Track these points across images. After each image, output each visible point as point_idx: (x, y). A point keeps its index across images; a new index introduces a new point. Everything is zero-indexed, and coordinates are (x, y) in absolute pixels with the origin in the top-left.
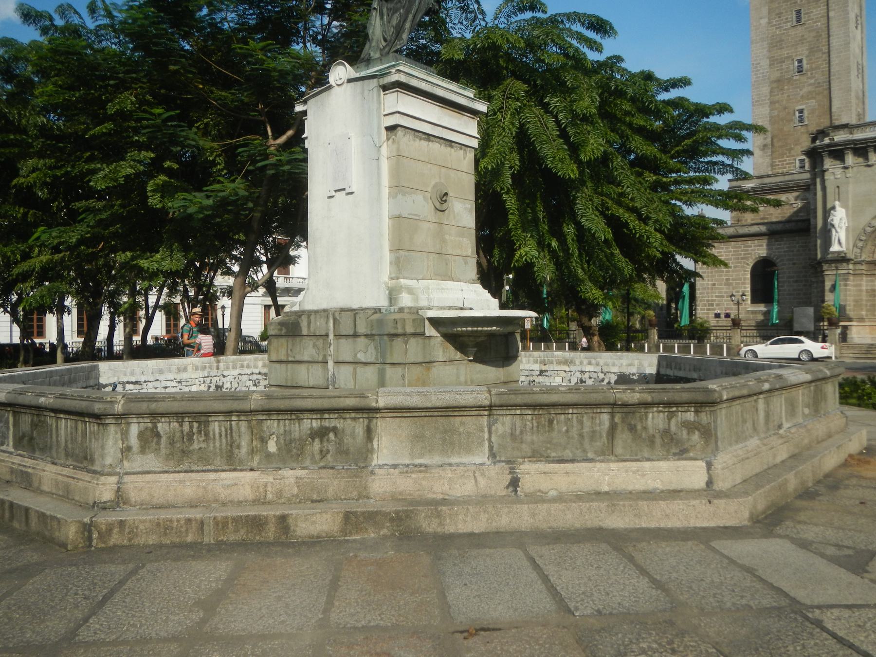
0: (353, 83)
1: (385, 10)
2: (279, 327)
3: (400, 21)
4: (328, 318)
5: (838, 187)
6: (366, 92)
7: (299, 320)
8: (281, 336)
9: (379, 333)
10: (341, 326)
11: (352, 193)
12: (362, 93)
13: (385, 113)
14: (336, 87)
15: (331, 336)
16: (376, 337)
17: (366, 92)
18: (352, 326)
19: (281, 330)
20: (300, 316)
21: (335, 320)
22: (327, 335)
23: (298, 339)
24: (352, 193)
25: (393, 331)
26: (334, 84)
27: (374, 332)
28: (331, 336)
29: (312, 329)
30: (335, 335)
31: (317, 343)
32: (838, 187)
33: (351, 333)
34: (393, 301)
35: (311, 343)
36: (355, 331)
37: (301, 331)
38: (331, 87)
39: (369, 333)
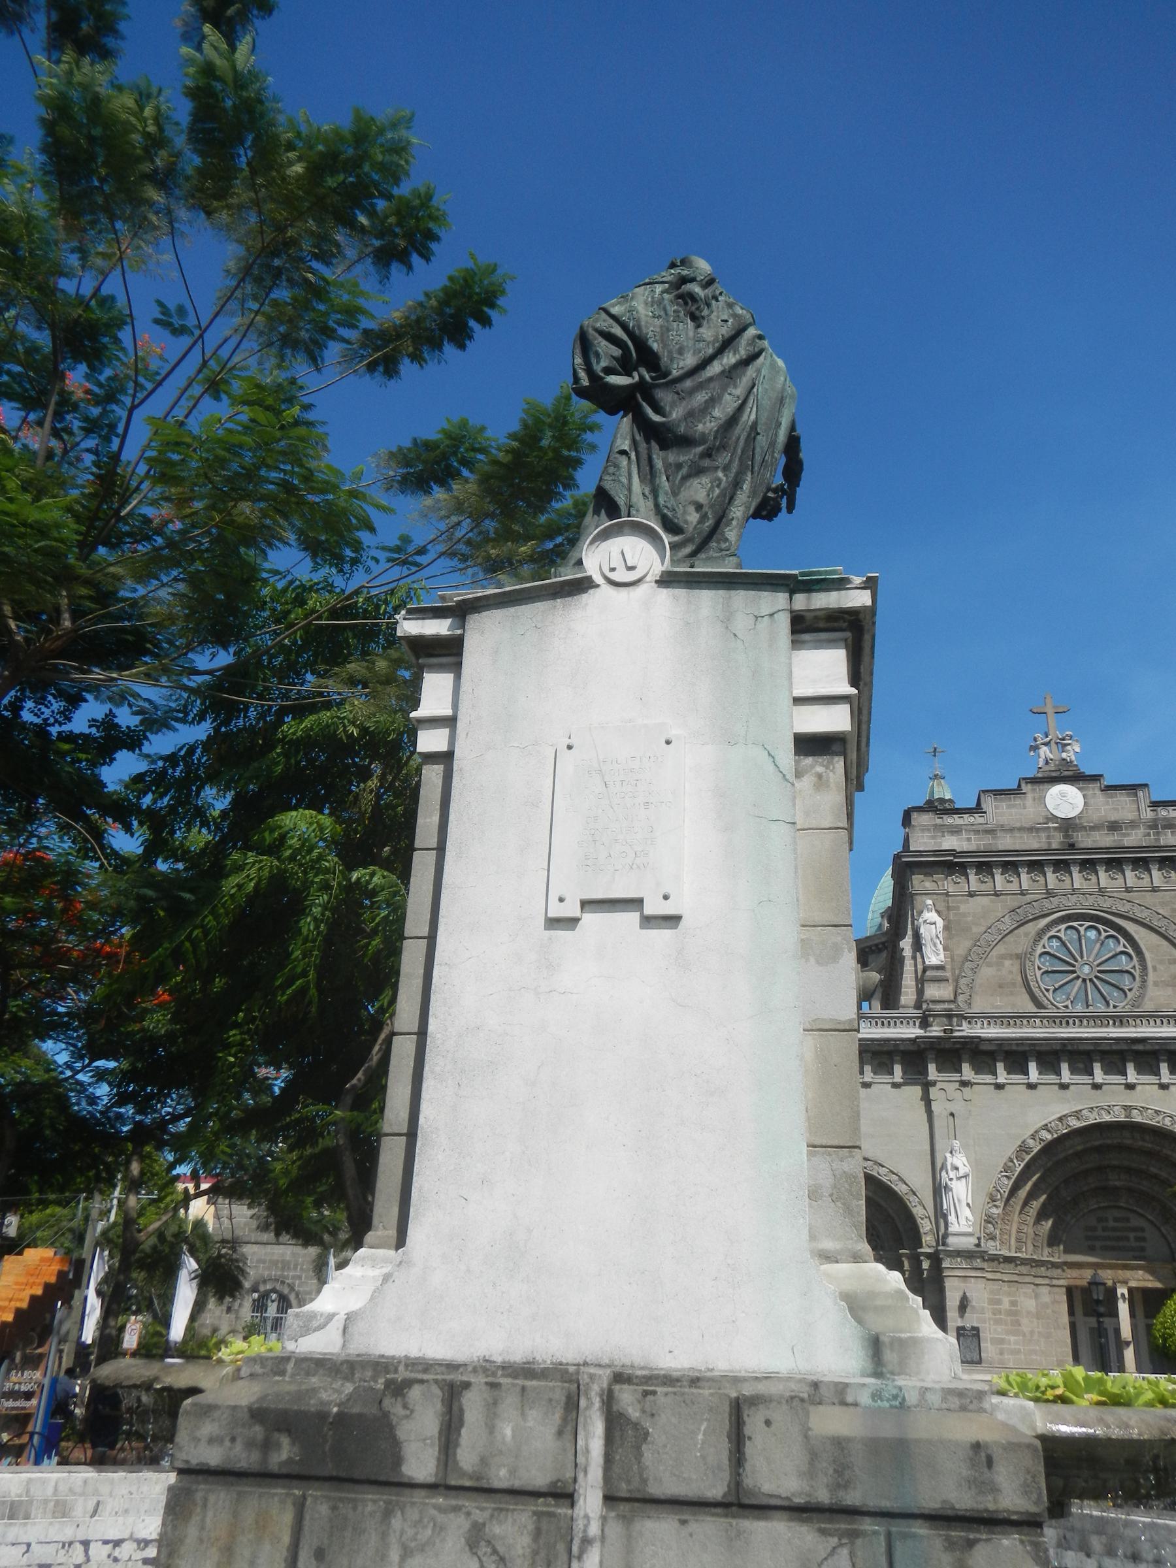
0: (681, 592)
1: (659, 464)
2: (258, 1431)
3: (723, 494)
4: (572, 1406)
5: (952, 1115)
6: (741, 623)
7: (395, 1408)
8: (263, 1476)
9: (886, 1504)
10: (648, 1455)
11: (672, 920)
12: (727, 620)
13: (798, 692)
14: (606, 589)
15: (590, 1501)
16: (867, 1525)
17: (741, 623)
18: (721, 1450)
19: (267, 1446)
20: (398, 1389)
21: (615, 1422)
22: (564, 1495)
23: (371, 1502)
24: (672, 920)
25: (964, 1500)
26: (598, 579)
27: (852, 1498)
28: (590, 1501)
29: (467, 1456)
30: (610, 1499)
31: (497, 1529)
32: (952, 1115)
33: (717, 1490)
34: (889, 1356)
35: (458, 1525)
36: (737, 1483)
37: (398, 1460)
38: (583, 585)
39: (823, 1496)
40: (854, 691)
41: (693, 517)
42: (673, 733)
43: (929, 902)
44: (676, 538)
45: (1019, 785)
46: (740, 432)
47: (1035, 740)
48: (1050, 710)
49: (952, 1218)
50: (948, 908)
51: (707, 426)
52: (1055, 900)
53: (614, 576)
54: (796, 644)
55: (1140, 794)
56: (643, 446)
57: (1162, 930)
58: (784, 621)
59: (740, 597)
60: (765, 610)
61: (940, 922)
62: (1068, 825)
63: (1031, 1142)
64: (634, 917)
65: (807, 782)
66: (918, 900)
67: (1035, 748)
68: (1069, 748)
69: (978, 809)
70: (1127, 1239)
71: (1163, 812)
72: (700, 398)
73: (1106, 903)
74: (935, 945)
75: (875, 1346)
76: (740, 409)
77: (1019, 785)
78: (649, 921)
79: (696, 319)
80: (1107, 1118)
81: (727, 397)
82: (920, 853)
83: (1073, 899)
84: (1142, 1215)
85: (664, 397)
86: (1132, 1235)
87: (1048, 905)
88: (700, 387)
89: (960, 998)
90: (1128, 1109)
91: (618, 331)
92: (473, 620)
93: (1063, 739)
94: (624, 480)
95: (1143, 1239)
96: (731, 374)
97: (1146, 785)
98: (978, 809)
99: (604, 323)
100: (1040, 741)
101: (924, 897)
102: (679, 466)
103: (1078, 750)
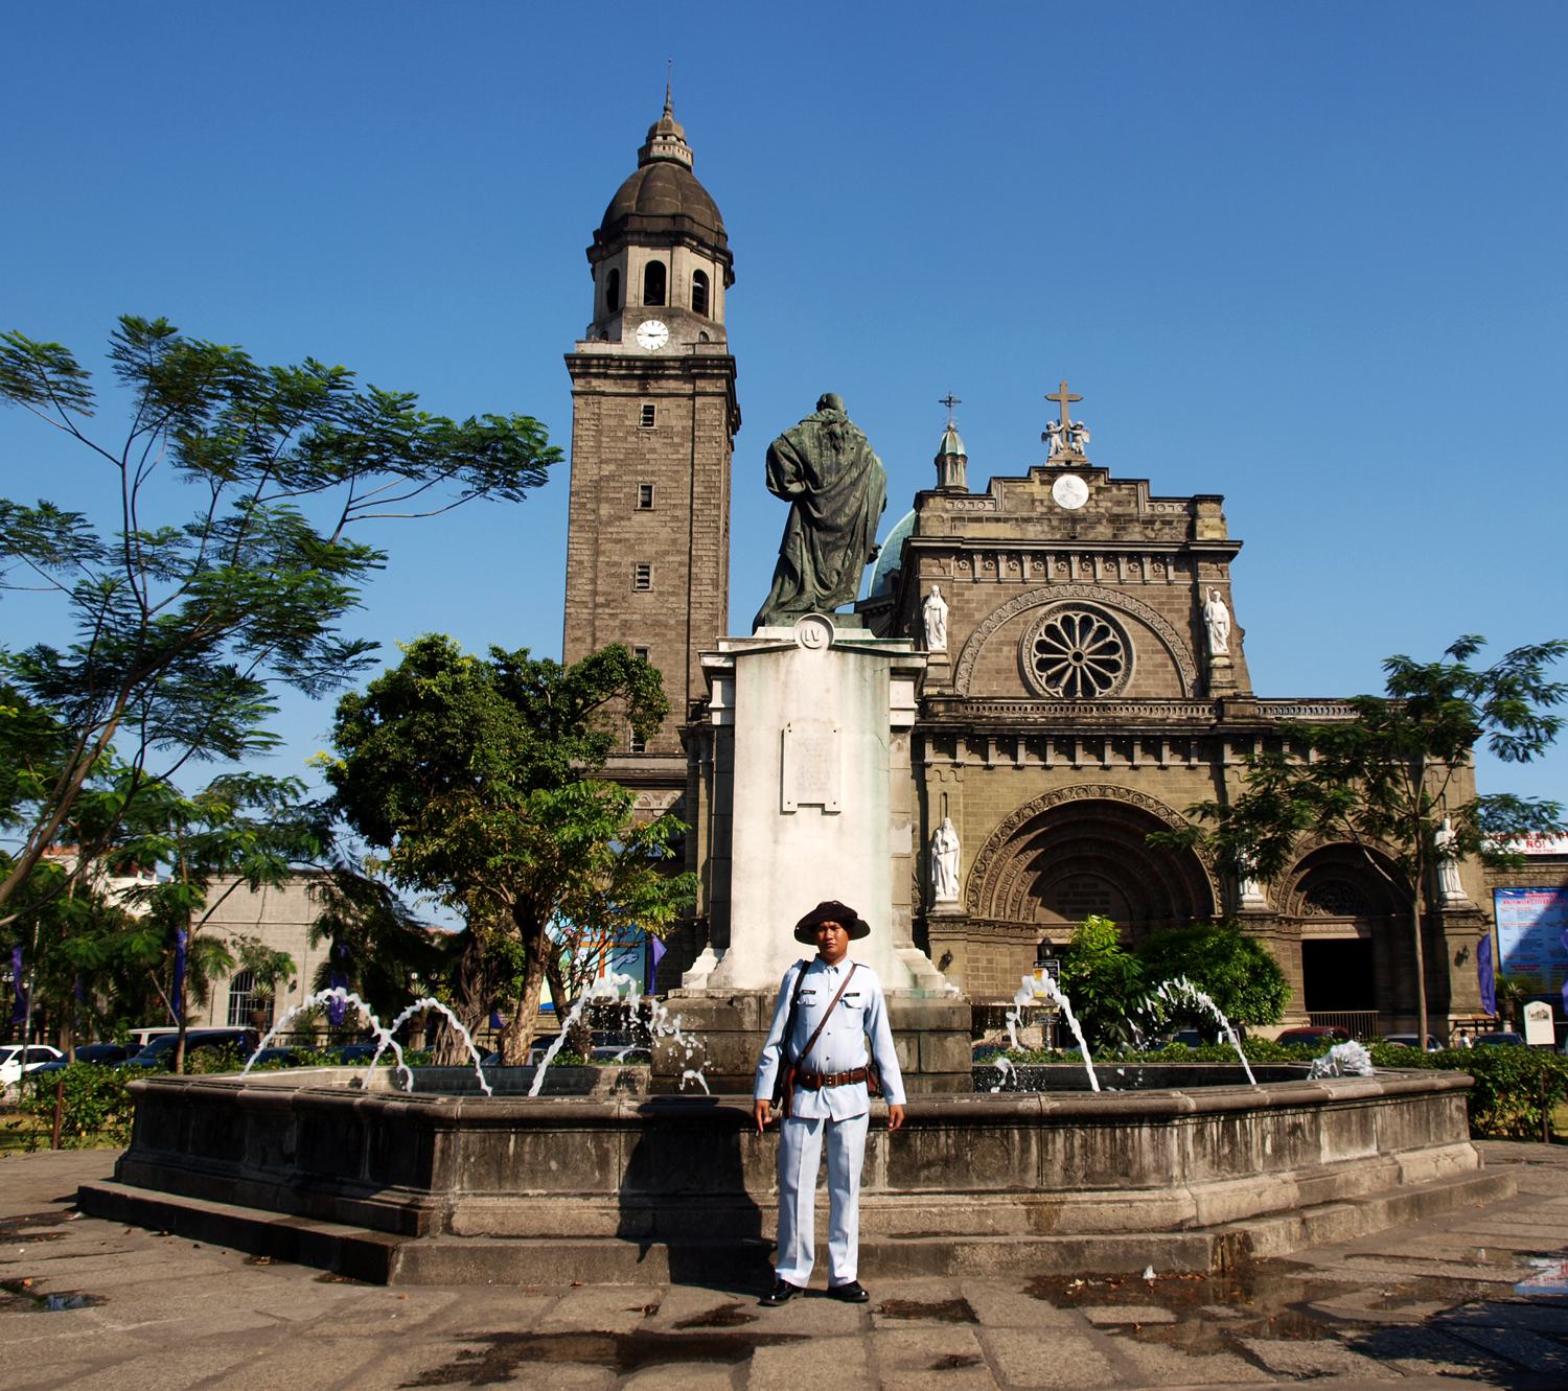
12: (862, 669)
26: (801, 645)
34: (920, 981)
40: (916, 706)
41: (835, 579)
42: (837, 726)
43: (936, 588)
44: (826, 593)
45: (1029, 474)
46: (860, 522)
47: (1048, 427)
48: (1064, 399)
49: (939, 888)
50: (953, 594)
51: (842, 520)
52: (1054, 590)
53: (807, 643)
54: (892, 679)
55: (1140, 488)
56: (807, 529)
57: (1148, 622)
58: (887, 672)
59: (868, 658)
60: (879, 668)
61: (945, 609)
62: (1072, 518)
63: (1016, 819)
64: (820, 810)
65: (894, 746)
66: (924, 584)
67: (1046, 436)
68: (1078, 438)
69: (988, 495)
70: (1094, 902)
71: (1159, 509)
72: (840, 500)
73: (1101, 594)
74: (938, 630)
75: (915, 978)
76: (860, 508)
77: (1029, 474)
78: (825, 813)
79: (837, 449)
80: (1084, 797)
81: (852, 499)
82: (929, 539)
83: (1071, 589)
84: (1108, 882)
85: (821, 501)
86: (1098, 899)
87: (1048, 594)
88: (839, 494)
89: (959, 683)
90: (1103, 789)
91: (794, 456)
92: (740, 660)
93: (1074, 429)
94: (798, 553)
95: (1108, 902)
96: (854, 483)
97: (1147, 481)
98: (988, 495)
99: (786, 449)
100: (1053, 429)
101: (930, 583)
102: (827, 544)
103: (1087, 440)
